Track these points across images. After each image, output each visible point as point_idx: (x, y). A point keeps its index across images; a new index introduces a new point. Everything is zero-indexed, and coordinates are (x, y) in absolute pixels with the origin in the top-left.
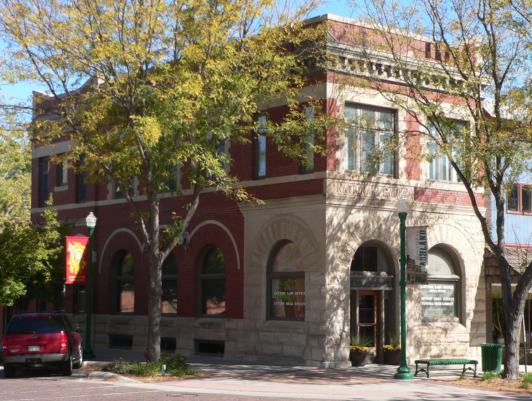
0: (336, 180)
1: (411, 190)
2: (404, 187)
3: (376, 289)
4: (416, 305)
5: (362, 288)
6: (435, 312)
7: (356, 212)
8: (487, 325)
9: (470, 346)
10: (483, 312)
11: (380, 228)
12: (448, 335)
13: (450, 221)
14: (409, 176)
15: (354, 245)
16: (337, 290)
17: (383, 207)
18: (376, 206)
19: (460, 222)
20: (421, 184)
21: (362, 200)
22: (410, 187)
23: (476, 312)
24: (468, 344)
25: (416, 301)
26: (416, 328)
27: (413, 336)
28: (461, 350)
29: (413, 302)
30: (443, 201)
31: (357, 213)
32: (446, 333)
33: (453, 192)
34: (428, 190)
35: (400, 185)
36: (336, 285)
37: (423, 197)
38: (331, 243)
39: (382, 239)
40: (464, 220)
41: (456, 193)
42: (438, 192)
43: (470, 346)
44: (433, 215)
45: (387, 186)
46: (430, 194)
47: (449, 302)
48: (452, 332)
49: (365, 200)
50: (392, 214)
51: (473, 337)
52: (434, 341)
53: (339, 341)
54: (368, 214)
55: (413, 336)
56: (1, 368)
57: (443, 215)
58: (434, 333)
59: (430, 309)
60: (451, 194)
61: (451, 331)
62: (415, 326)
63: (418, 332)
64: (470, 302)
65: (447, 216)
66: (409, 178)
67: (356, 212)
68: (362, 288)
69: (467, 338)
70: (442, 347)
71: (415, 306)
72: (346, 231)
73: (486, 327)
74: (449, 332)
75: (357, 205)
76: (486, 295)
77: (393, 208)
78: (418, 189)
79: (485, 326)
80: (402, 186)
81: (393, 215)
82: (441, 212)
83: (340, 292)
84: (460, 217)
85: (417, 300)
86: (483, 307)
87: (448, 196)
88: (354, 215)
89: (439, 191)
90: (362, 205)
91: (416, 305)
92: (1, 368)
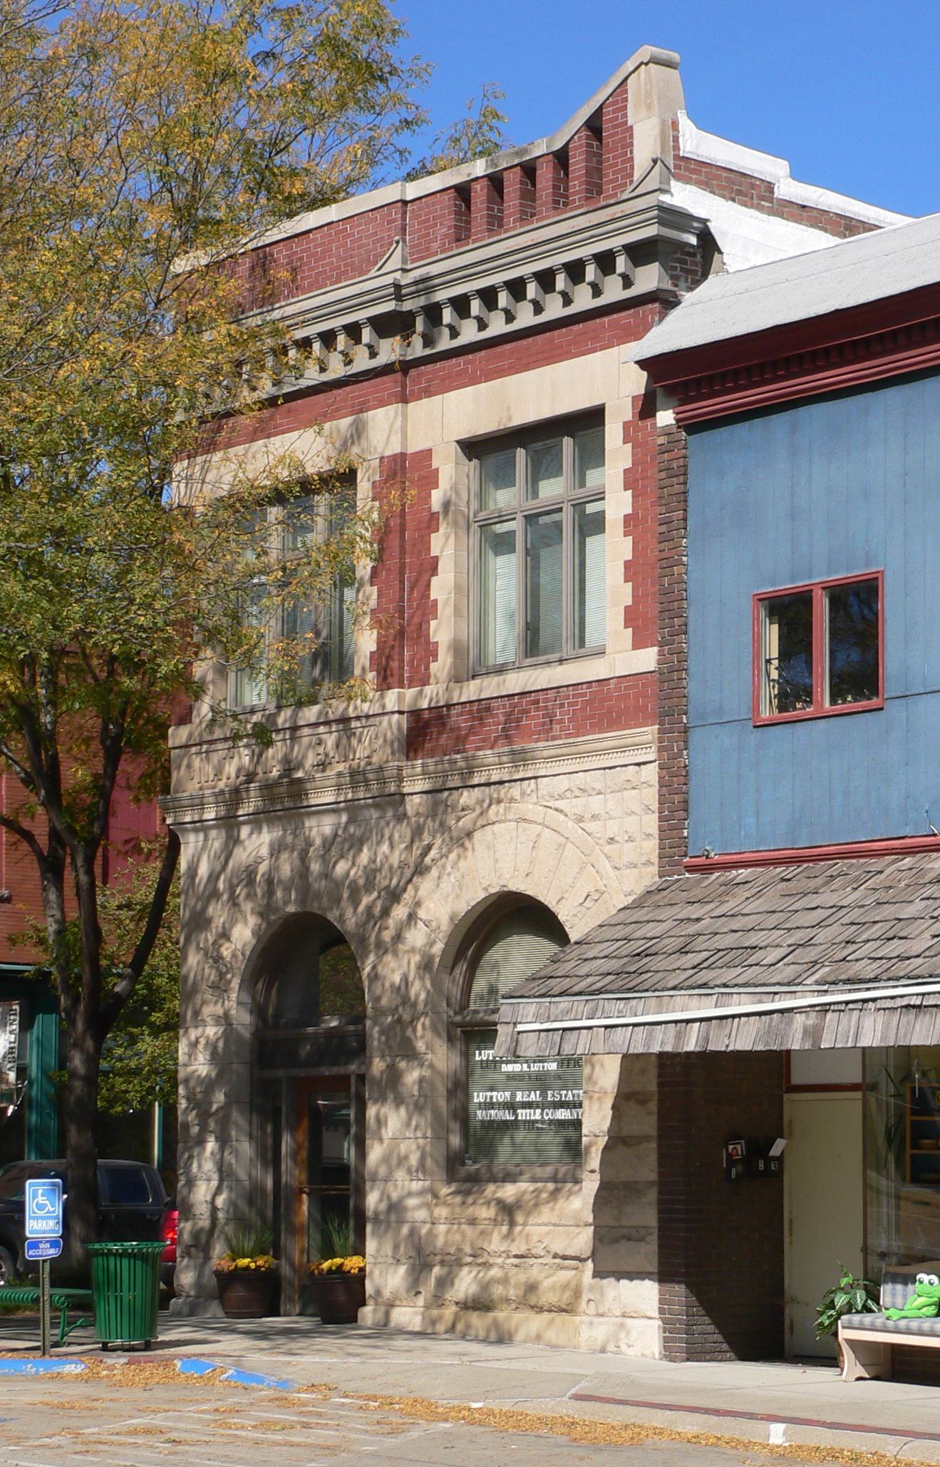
0: (194, 750)
1: (394, 725)
2: (372, 721)
3: (335, 1070)
4: (414, 1123)
5: (296, 1072)
6: (536, 1144)
7: (251, 833)
8: (660, 1193)
9: (598, 1274)
10: (646, 1138)
11: (303, 872)
12: (518, 1229)
13: (528, 808)
14: (385, 678)
15: (244, 934)
16: (201, 1081)
17: (305, 804)
18: (288, 804)
19: (559, 804)
20: (431, 695)
21: (244, 795)
22: (386, 718)
23: (617, 1140)
24: (590, 1265)
25: (411, 1107)
26: (412, 1202)
27: (405, 1230)
28: (553, 1288)
29: (403, 1111)
30: (508, 737)
31: (254, 836)
32: (512, 1224)
33: (541, 696)
34: (458, 709)
35: (358, 718)
36: (201, 1066)
37: (443, 740)
38: (193, 937)
39: (314, 907)
40: (577, 793)
41: (551, 694)
42: (488, 709)
43: (598, 1274)
44: (466, 798)
45: (322, 729)
46: (466, 721)
47: (490, 1105)
48: (531, 1220)
49: (252, 794)
50: (344, 818)
51: (601, 1241)
52: (468, 1250)
53: (203, 1238)
54: (281, 833)
55: (405, 1230)
56: (2, 1283)
57: (503, 790)
58: (473, 1222)
59: (520, 1136)
60: (536, 702)
61: (528, 1214)
62: (410, 1194)
63: (421, 1214)
64: (596, 1106)
65: (515, 790)
66: (385, 686)
67: (251, 833)
68: (296, 1072)
69: (583, 1240)
70: (494, 1272)
71: (408, 1124)
72: (225, 897)
73: (660, 1202)
74: (520, 1218)
75: (240, 812)
76: (660, 1075)
77: (331, 799)
78: (426, 715)
79: (653, 1195)
80: (364, 721)
81: (347, 823)
82: (495, 778)
83: (210, 1085)
84: (563, 783)
85: (416, 1105)
86: (646, 1123)
87: (526, 712)
88: (247, 843)
89: (494, 704)
90: (251, 810)
91: (414, 1123)
92: (2, 1283)
